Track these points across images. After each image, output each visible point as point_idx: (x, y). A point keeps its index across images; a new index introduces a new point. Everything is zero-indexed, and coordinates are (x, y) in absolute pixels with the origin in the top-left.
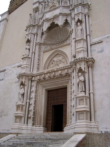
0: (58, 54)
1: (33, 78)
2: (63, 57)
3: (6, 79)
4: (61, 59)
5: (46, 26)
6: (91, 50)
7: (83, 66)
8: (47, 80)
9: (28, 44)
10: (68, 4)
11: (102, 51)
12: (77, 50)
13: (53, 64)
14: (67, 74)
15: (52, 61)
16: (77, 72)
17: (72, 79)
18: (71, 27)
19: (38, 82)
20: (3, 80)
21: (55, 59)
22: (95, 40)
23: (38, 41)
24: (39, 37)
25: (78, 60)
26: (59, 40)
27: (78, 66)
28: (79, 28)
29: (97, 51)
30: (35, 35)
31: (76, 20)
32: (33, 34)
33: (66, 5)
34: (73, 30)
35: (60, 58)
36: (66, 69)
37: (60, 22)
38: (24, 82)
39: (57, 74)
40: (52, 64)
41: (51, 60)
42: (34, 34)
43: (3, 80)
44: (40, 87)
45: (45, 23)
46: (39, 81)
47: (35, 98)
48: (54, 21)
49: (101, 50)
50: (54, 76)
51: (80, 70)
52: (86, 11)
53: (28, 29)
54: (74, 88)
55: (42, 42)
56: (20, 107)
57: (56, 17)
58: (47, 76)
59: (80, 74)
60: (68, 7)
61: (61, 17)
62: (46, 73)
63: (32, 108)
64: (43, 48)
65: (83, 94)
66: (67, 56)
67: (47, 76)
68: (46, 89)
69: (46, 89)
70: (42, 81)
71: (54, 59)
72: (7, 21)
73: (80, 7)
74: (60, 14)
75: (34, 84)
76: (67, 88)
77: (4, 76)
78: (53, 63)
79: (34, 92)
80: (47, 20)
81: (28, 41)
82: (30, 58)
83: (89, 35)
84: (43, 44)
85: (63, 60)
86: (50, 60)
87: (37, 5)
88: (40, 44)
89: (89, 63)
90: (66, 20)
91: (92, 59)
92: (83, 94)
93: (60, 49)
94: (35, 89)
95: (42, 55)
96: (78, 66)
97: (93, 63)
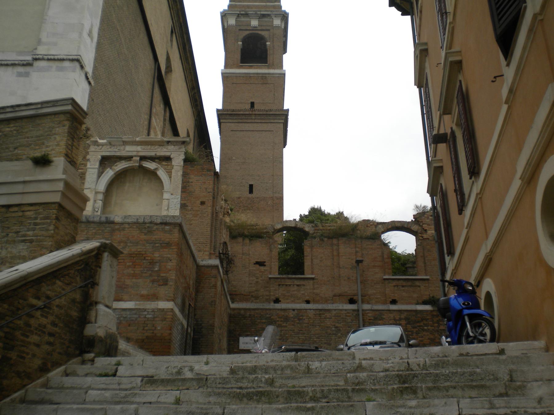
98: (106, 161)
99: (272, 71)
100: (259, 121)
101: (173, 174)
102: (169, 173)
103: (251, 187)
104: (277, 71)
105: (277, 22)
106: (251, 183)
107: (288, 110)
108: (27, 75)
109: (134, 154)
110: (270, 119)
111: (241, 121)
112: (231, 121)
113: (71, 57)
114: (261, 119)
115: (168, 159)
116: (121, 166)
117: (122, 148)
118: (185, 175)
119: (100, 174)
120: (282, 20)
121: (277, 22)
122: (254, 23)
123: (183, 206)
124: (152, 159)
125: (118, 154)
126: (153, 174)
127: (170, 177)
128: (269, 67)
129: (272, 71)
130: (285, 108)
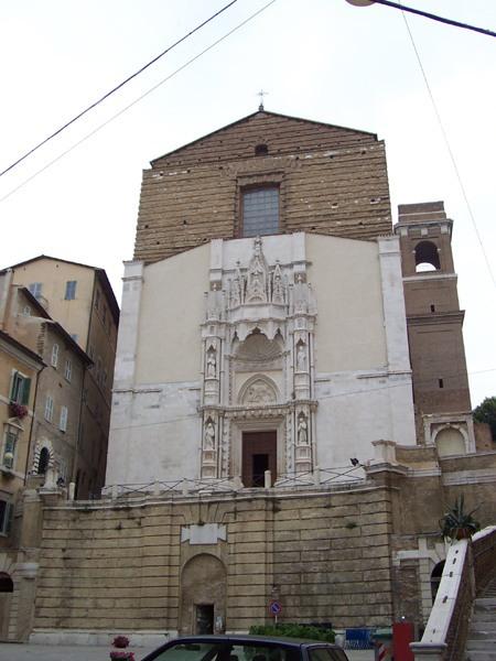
5: (243, 332)
7: (306, 411)
10: (282, 304)
20: (158, 407)
21: (255, 387)
22: (321, 376)
23: (228, 353)
24: (229, 346)
27: (299, 410)
33: (277, 303)
35: (264, 387)
37: (270, 332)
39: (264, 413)
43: (158, 407)
44: (235, 427)
45: (241, 325)
47: (230, 443)
50: (261, 415)
51: (302, 415)
53: (209, 327)
54: (290, 435)
60: (282, 307)
61: (270, 323)
63: (226, 457)
64: (234, 363)
65: (304, 444)
66: (276, 387)
67: (249, 414)
72: (143, 282)
73: (304, 319)
75: (227, 422)
76: (275, 432)
80: (247, 322)
85: (269, 391)
86: (247, 389)
87: (217, 277)
88: (230, 358)
90: (279, 331)
92: (304, 444)
93: (265, 373)
96: (299, 410)
98: (433, 426)
99: (446, 276)
102: (466, 429)
103: (441, 381)
104: (450, 276)
105: (444, 229)
107: (464, 311)
108: (384, 382)
115: (465, 422)
116: (440, 428)
122: (424, 232)
123: (477, 448)
124: (456, 423)
126: (458, 430)
128: (443, 272)
129: (446, 276)
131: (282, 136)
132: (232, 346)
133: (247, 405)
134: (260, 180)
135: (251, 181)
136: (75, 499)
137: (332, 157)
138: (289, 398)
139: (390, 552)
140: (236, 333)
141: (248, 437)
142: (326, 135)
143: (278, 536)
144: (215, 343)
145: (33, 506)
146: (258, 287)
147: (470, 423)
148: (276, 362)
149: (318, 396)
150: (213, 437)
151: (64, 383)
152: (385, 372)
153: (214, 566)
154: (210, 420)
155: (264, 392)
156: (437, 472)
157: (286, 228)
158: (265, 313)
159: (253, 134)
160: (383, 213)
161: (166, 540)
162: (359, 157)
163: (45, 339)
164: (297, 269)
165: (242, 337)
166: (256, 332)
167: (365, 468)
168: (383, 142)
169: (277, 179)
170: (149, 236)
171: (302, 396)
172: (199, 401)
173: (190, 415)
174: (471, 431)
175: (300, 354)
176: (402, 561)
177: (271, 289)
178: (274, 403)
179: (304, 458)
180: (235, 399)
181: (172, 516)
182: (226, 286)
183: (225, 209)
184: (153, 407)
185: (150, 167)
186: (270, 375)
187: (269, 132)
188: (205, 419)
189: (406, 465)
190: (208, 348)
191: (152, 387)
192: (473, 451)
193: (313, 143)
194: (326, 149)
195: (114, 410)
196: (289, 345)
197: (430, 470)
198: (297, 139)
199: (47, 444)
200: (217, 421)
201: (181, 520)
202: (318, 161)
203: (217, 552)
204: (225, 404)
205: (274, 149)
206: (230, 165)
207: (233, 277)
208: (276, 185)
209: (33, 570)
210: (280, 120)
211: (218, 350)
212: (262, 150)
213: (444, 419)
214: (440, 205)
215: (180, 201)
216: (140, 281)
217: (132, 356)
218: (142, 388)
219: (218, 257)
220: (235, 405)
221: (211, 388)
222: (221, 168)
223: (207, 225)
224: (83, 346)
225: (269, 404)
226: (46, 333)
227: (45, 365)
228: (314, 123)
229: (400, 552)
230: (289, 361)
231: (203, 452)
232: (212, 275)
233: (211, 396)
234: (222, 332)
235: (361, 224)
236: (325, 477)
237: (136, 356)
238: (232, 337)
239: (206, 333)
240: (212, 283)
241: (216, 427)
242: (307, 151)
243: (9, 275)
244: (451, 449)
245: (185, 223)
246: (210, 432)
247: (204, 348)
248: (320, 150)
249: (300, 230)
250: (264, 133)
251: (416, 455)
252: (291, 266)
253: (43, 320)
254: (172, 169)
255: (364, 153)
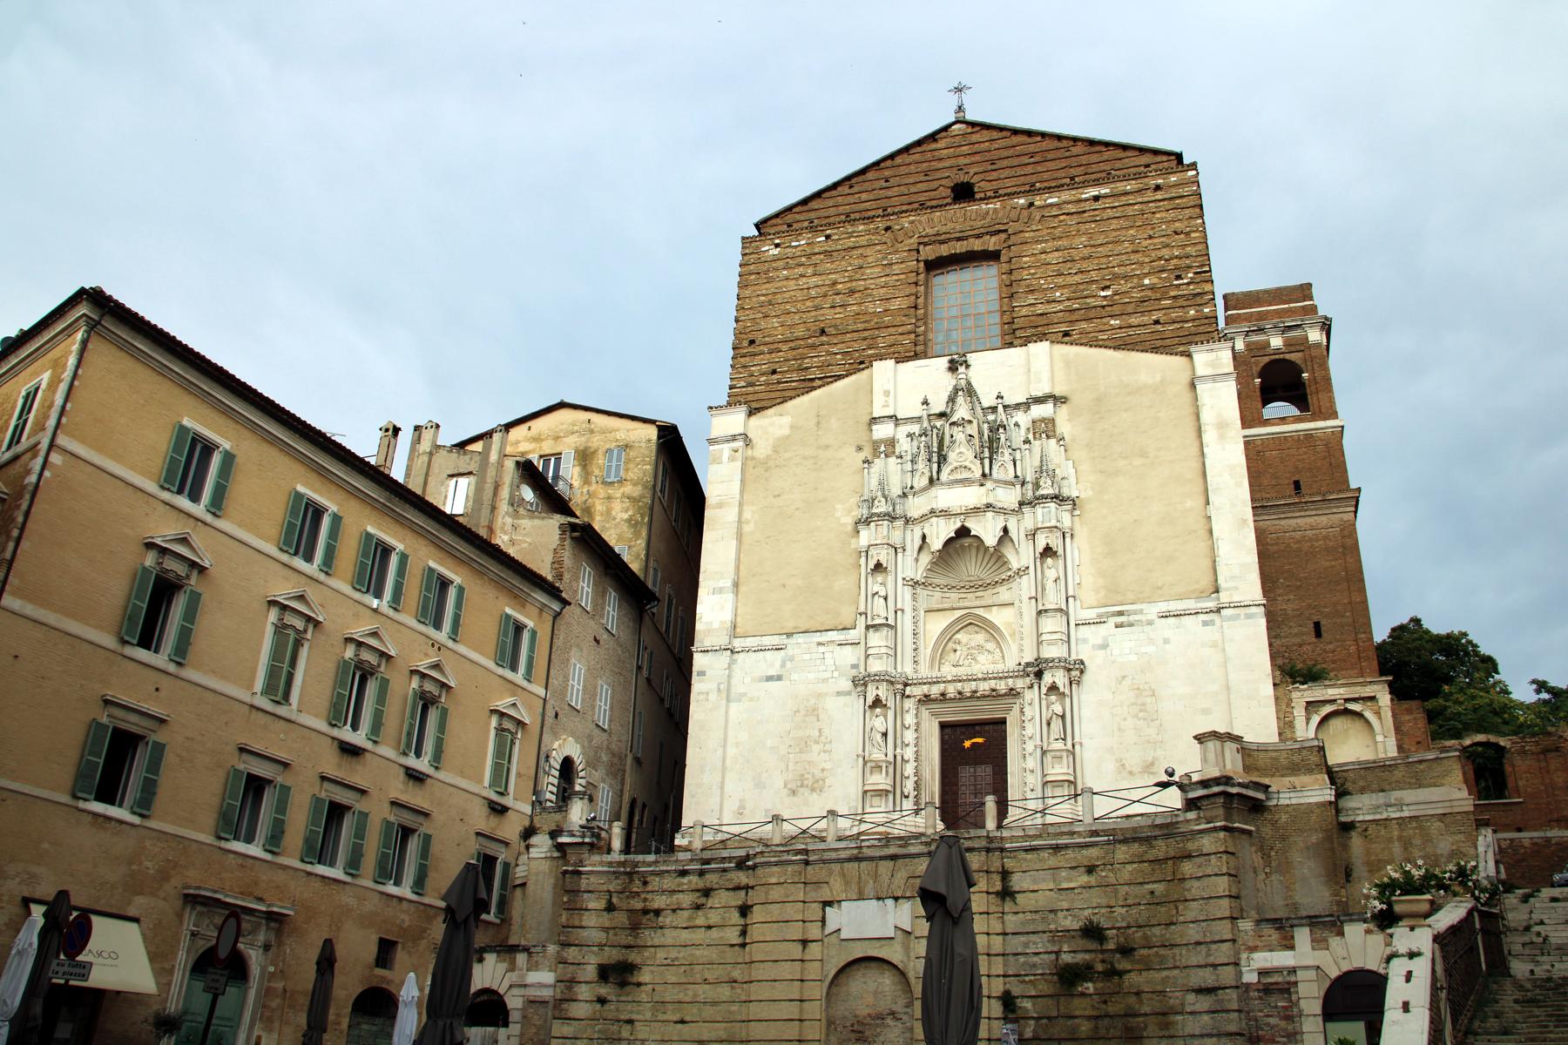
0: (971, 624)
1: (908, 688)
2: (988, 636)
3: (795, 677)
4: (982, 642)
5: (941, 532)
6: (1077, 640)
7: (1060, 678)
8: (951, 699)
9: (880, 578)
11: (1104, 646)
12: (1044, 637)
13: (958, 652)
14: (1012, 689)
15: (952, 640)
16: (1044, 690)
17: (1026, 705)
18: (1017, 553)
19: (919, 700)
20: (779, 678)
23: (910, 574)
25: (1050, 664)
26: (972, 579)
27: (1048, 678)
28: (1051, 574)
29: (1091, 643)
30: (899, 550)
31: (1041, 547)
32: (892, 547)
34: (1028, 568)
35: (980, 638)
36: (1011, 677)
37: (989, 535)
38: (883, 700)
39: (984, 687)
40: (955, 651)
41: (950, 639)
42: (896, 549)
44: (925, 713)
46: (926, 700)
48: (967, 524)
49: (1100, 641)
51: (1053, 688)
52: (1066, 520)
55: (918, 577)
56: (881, 767)
57: (976, 511)
58: (951, 690)
59: (1053, 698)
62: (949, 682)
63: (909, 769)
65: (1059, 745)
67: (951, 690)
68: (940, 722)
69: (940, 722)
70: (934, 700)
71: (957, 636)
73: (1053, 505)
74: (989, 506)
75: (909, 704)
76: (1003, 722)
77: (783, 665)
78: (958, 648)
79: (913, 728)
80: (945, 514)
81: (878, 567)
82: (888, 626)
83: (1074, 597)
84: (923, 583)
85: (991, 646)
86: (948, 635)
87: (883, 431)
88: (915, 584)
89: (1073, 673)
90: (1005, 530)
91: (1082, 662)
94: (915, 721)
95: (922, 620)
97: (1082, 672)
98: (1311, 706)
100: (1314, 513)
101: (1383, 714)
102: (1378, 713)
103: (1317, 625)
105: (1315, 335)
106: (1316, 619)
107: (1359, 490)
108: (1212, 623)
109: (1338, 697)
110: (1332, 508)
111: (1283, 516)
112: (1266, 517)
113: (1257, 603)
114: (1316, 509)
115: (1372, 698)
116: (1328, 709)
117: (1324, 692)
118: (1394, 716)
119: (1308, 720)
120: (1322, 329)
121: (1315, 335)
122: (1276, 342)
123: (1400, 748)
124: (1355, 700)
125: (1322, 699)
127: (1380, 718)
130: (1353, 485)
131: (1000, 164)
132: (917, 560)
133: (948, 671)
134: (959, 248)
135: (944, 250)
136: (626, 850)
137: (1096, 198)
138: (1029, 657)
139: (1237, 953)
140: (924, 537)
141: (951, 733)
142: (1084, 160)
143: (1012, 922)
144: (883, 555)
145: (545, 866)
146: (962, 454)
147: (1385, 699)
148: (1002, 589)
149: (1086, 645)
150: (885, 735)
151: (604, 637)
152: (1211, 604)
153: (888, 982)
154: (877, 703)
155: (980, 647)
156: (1328, 795)
157: (1014, 334)
158: (972, 496)
159: (947, 164)
160: (1199, 300)
161: (796, 932)
162: (1149, 196)
163: (567, 556)
164: (1038, 411)
165: (937, 544)
166: (963, 532)
167: (1181, 787)
168: (1193, 166)
169: (992, 243)
170: (757, 360)
171: (1050, 652)
172: (854, 666)
173: (839, 694)
174: (1387, 714)
175: (1047, 572)
176: (1263, 973)
177: (990, 445)
178: (1000, 667)
179: (1059, 771)
180: (926, 653)
181: (805, 883)
182: (904, 445)
183: (895, 305)
184: (769, 679)
185: (757, 233)
186: (996, 616)
187: (977, 158)
188: (870, 700)
189: (1266, 781)
190: (871, 565)
191: (768, 641)
192: (1393, 752)
193: (1062, 174)
194: (1086, 184)
195: (697, 686)
196: (1021, 555)
197: (1318, 792)
198: (1029, 169)
199: (573, 749)
200: (890, 704)
201: (826, 895)
202: (1072, 208)
203: (894, 954)
204: (908, 669)
205: (981, 187)
206: (905, 222)
207: (916, 428)
208: (992, 256)
209: (542, 985)
210: (995, 135)
211: (891, 568)
212: (964, 193)
213: (1331, 693)
214: (1305, 291)
215: (813, 292)
216: (739, 444)
217: (728, 583)
218: (750, 642)
219: (887, 393)
220: (925, 672)
221: (877, 640)
222: (887, 229)
223: (866, 334)
224: (635, 567)
225: (991, 668)
226: (568, 542)
227: (565, 603)
228: (1059, 138)
229: (1256, 955)
230: (1026, 585)
231: (865, 763)
232: (874, 427)
233: (879, 656)
234: (896, 537)
235: (1157, 322)
236: (1102, 807)
237: (736, 585)
238: (918, 542)
239: (866, 536)
240: (875, 445)
241: (890, 714)
242: (1050, 190)
243: (496, 437)
244: (1347, 748)
245: (823, 332)
246: (879, 724)
247: (866, 565)
248: (1073, 184)
249: (1041, 337)
250: (967, 161)
251: (1285, 762)
252: (1025, 406)
253: (558, 520)
254: (798, 234)
255: (1158, 188)
